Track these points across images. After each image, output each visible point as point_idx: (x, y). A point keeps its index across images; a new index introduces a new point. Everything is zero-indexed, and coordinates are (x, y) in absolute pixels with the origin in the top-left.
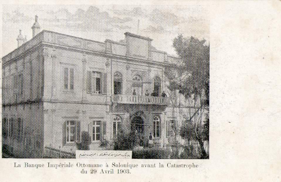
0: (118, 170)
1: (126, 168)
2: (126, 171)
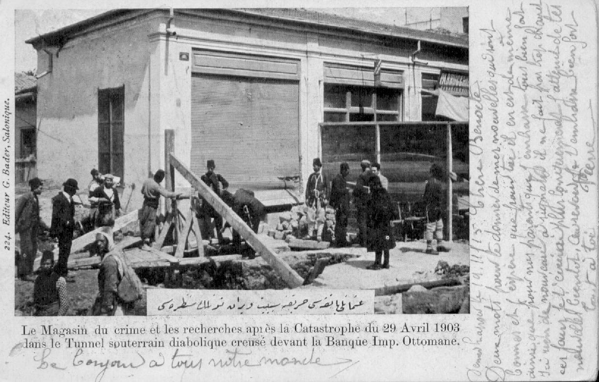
0: (437, 325)
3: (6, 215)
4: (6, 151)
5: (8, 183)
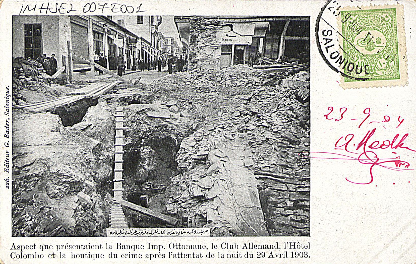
0: (292, 252)
1: (303, 250)
2: (304, 254)
3: (7, 166)
4: (7, 122)
5: (8, 144)
